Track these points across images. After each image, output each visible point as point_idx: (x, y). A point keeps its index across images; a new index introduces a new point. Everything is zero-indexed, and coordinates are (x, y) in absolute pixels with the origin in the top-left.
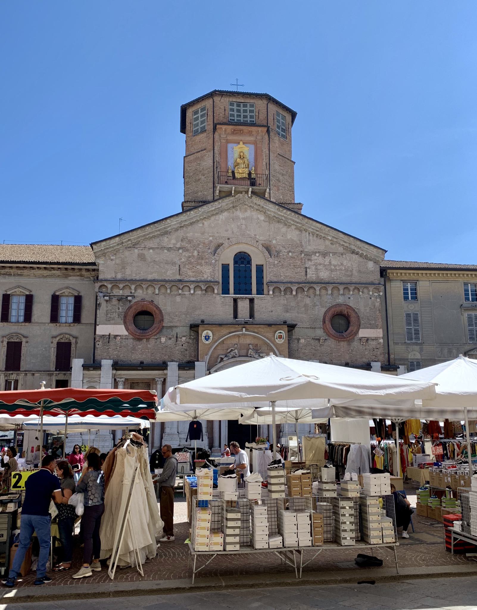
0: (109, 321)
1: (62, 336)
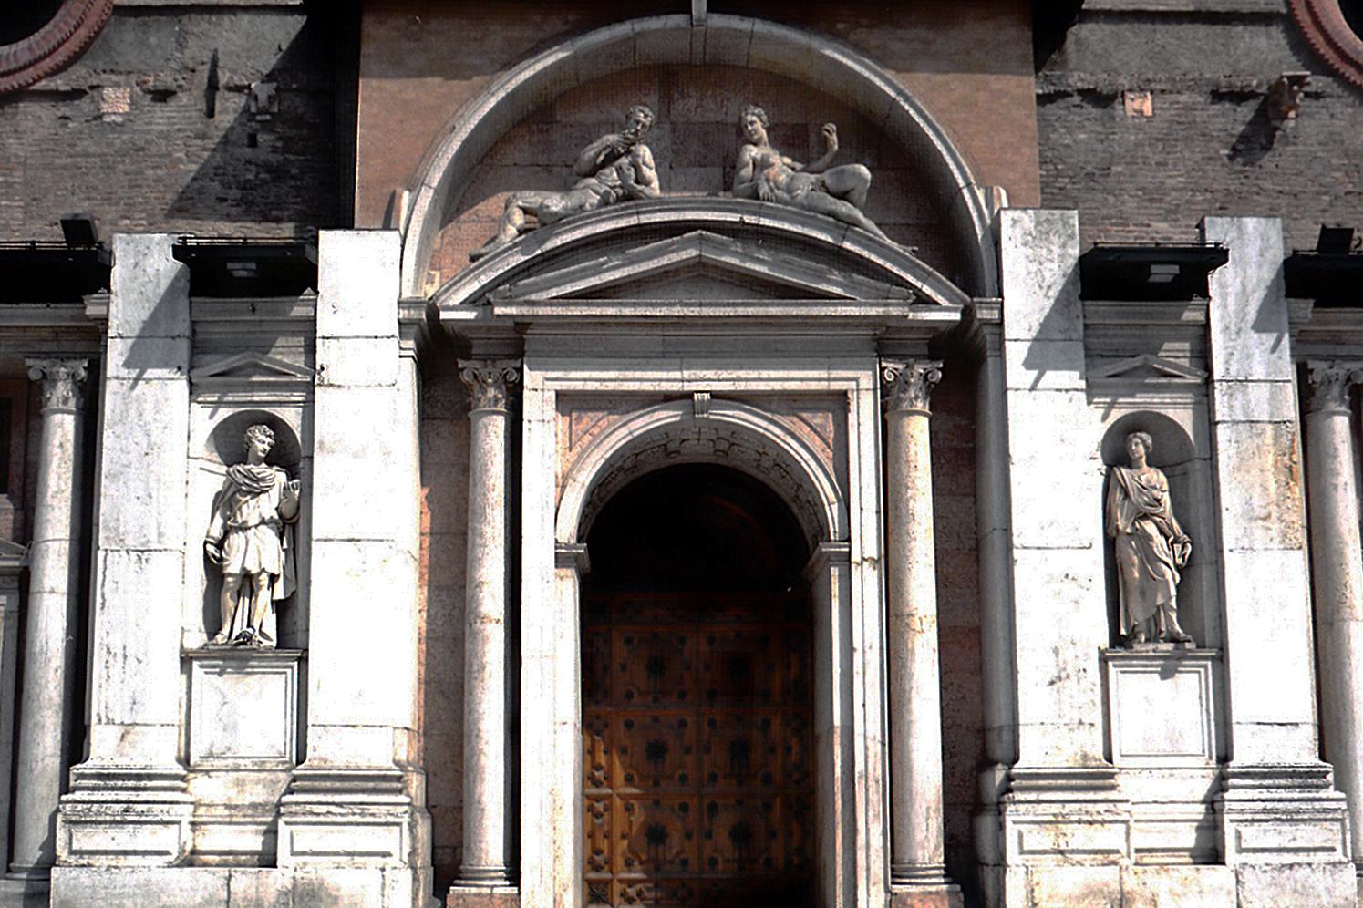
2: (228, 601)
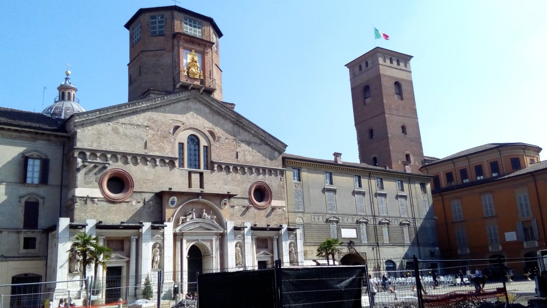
0: (87, 184)
1: (29, 196)
2: (155, 264)
